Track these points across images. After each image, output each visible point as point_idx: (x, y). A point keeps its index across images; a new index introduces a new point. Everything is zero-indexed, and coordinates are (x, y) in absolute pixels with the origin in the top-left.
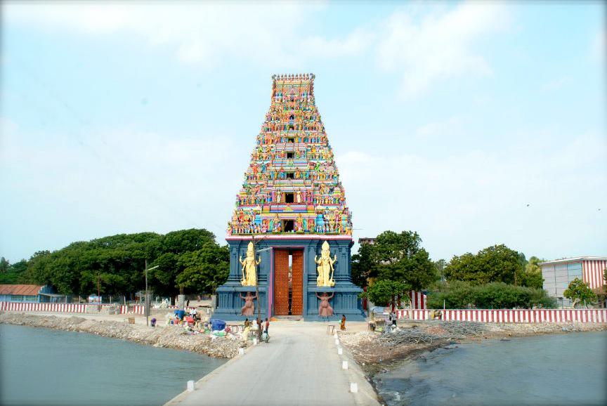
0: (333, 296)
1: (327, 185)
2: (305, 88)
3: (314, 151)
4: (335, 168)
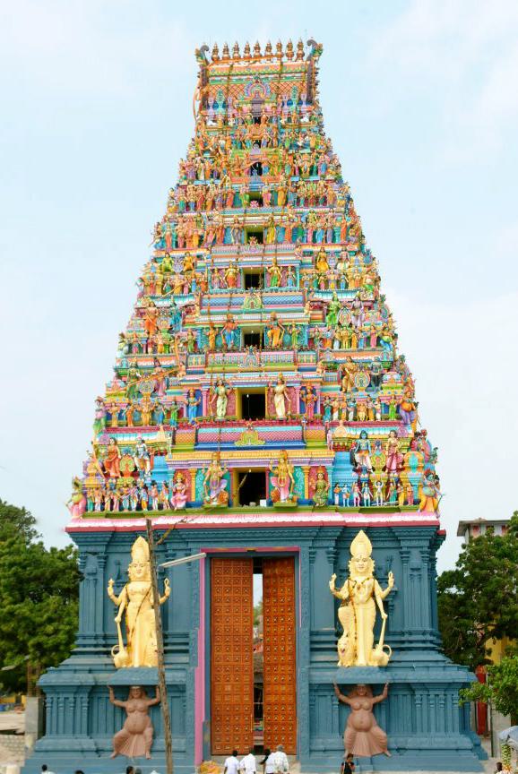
0: (385, 695)
1: (362, 367)
2: (293, 84)
3: (323, 267)
4: (386, 315)
